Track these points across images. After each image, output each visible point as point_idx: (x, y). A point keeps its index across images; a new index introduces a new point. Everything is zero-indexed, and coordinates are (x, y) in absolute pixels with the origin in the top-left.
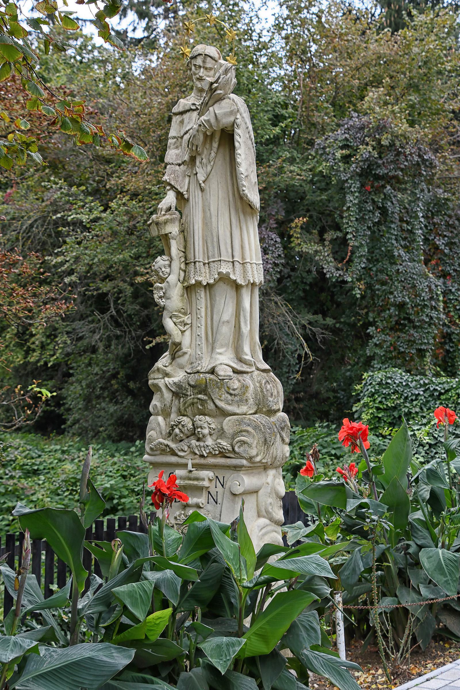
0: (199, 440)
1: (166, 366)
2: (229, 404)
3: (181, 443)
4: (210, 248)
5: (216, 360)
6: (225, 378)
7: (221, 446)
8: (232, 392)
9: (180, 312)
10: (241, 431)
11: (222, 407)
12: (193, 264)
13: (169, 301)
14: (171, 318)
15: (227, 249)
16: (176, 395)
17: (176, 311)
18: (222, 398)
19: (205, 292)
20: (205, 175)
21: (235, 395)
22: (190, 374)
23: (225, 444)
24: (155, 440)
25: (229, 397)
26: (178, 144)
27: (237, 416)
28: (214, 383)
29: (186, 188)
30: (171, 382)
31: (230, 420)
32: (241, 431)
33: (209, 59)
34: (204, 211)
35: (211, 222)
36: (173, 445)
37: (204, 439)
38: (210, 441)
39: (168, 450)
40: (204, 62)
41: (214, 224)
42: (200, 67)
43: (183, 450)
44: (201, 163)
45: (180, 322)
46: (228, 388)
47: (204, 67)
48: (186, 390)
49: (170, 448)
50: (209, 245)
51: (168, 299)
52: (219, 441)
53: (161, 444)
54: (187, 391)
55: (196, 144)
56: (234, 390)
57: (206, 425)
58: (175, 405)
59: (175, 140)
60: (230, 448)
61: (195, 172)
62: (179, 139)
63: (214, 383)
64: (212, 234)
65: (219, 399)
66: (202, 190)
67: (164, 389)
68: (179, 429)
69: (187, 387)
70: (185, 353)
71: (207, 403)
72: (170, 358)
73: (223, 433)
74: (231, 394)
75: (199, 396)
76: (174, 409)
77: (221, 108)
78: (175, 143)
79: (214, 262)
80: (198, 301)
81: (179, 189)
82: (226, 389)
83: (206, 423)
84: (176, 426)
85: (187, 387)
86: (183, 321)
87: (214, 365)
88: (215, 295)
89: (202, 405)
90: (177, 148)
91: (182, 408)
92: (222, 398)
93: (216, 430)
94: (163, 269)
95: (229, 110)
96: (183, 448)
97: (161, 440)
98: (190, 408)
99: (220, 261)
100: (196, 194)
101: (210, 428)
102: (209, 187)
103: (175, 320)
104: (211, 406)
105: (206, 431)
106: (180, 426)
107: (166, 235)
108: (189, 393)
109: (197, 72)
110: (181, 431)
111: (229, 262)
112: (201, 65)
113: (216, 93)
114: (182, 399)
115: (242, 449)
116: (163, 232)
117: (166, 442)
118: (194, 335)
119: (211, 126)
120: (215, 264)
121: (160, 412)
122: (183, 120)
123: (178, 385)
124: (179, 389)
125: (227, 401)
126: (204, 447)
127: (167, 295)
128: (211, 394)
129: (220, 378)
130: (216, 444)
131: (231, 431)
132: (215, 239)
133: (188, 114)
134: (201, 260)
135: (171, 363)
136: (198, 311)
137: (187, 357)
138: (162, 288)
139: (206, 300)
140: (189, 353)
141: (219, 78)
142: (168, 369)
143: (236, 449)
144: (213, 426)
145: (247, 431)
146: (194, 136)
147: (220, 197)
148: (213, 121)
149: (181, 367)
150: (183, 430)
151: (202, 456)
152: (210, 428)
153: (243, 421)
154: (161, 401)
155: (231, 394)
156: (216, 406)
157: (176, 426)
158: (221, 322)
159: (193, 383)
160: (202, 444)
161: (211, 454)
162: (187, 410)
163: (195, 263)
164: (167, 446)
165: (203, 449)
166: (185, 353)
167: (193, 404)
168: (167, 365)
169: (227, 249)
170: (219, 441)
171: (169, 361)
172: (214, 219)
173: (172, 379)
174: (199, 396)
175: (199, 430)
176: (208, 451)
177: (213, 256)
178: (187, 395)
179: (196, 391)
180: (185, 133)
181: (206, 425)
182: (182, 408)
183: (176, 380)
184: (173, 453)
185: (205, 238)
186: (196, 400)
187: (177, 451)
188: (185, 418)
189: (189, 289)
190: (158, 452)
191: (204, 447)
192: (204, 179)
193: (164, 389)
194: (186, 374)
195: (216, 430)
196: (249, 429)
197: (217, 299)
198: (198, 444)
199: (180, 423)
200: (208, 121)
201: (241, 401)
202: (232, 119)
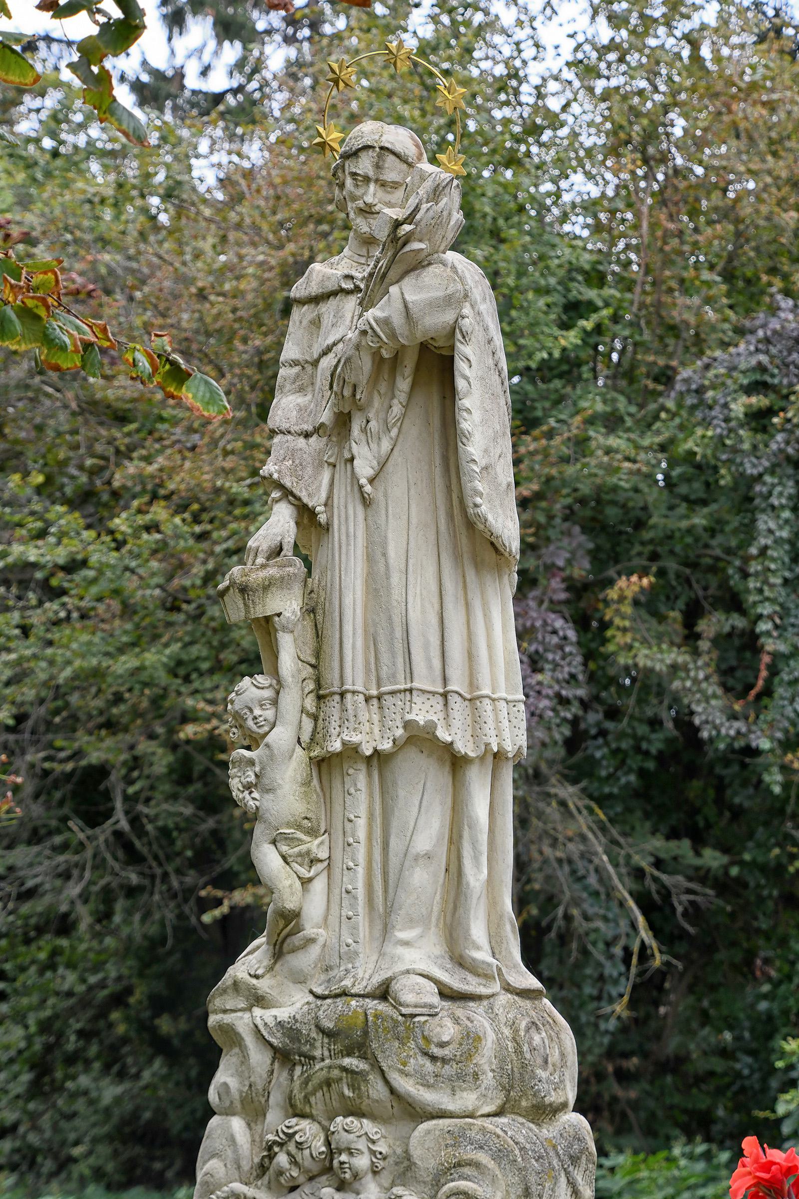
1: (256, 977)
2: (428, 1086)
4: (385, 658)
5: (394, 959)
8: (436, 1051)
9: (299, 827)
10: (459, 1165)
12: (337, 698)
13: (270, 796)
14: (274, 842)
15: (428, 660)
16: (283, 1056)
17: (288, 825)
18: (409, 1069)
19: (369, 775)
20: (375, 464)
21: (444, 1061)
25: (428, 1065)
26: (306, 380)
27: (447, 1121)
28: (389, 1024)
29: (323, 495)
31: (428, 1132)
32: (459, 1165)
33: (391, 158)
34: (370, 559)
35: (388, 588)
37: (356, 1185)
40: (378, 167)
41: (397, 594)
42: (367, 179)
44: (364, 430)
45: (300, 855)
46: (427, 1039)
47: (377, 181)
48: (312, 1043)
50: (383, 648)
54: (313, 1046)
56: (442, 1045)
57: (362, 1145)
58: (279, 1085)
59: (297, 369)
61: (347, 455)
62: (309, 368)
63: (389, 1024)
64: (390, 618)
65: (401, 1072)
66: (366, 502)
67: (249, 1041)
68: (289, 1154)
69: (314, 1035)
70: (312, 941)
71: (366, 1081)
72: (270, 953)
74: (433, 1058)
75: (347, 1061)
76: (276, 1098)
77: (421, 289)
78: (298, 376)
79: (392, 693)
81: (305, 500)
82: (421, 1041)
84: (281, 1145)
85: (314, 1035)
86: (308, 852)
87: (389, 974)
88: (395, 783)
89: (353, 1087)
90: (301, 390)
91: (299, 1096)
92: (409, 1069)
93: (391, 1160)
94: (257, 712)
95: (440, 294)
97: (238, 1187)
98: (319, 1094)
99: (411, 690)
101: (373, 1153)
102: (386, 496)
103: (284, 848)
105: (362, 1162)
106: (292, 1147)
107: (268, 619)
108: (317, 1053)
109: (359, 192)
110: (294, 1162)
111: (434, 693)
112: (371, 173)
113: (407, 248)
114: (298, 1070)
116: (259, 612)
119: (393, 335)
120: (398, 700)
121: (238, 1104)
122: (319, 317)
123: (289, 1030)
124: (292, 1040)
125: (423, 1077)
127: (265, 781)
128: (380, 1057)
129: (404, 1011)
131: (432, 1164)
132: (399, 633)
133: (333, 302)
134: (356, 688)
135: (271, 969)
136: (348, 826)
137: (314, 951)
138: (251, 763)
139: (371, 795)
140: (321, 941)
141: (417, 209)
142: (264, 985)
145: (477, 1165)
146: (348, 360)
147: (414, 520)
148: (398, 321)
149: (299, 979)
150: (299, 1158)
152: (373, 1153)
153: (464, 1135)
155: (433, 1058)
156: (392, 1091)
157: (281, 1145)
158: (410, 857)
159: (331, 1025)
162: (313, 1100)
163: (342, 695)
166: (312, 941)
167: (328, 1083)
168: (260, 972)
169: (428, 660)
171: (266, 962)
172: (396, 579)
173: (274, 1012)
174: (347, 1061)
175: (344, 1157)
177: (393, 678)
178: (313, 1058)
179: (338, 1047)
180: (325, 353)
181: (362, 1145)
182: (299, 1096)
183: (283, 1013)
185: (372, 630)
186: (336, 1073)
188: (305, 1124)
189: (326, 766)
192: (370, 472)
193: (249, 1041)
194: (311, 998)
195: (391, 1160)
196: (483, 1157)
197: (402, 793)
199: (291, 1136)
200: (385, 322)
201: (461, 1076)
202: (449, 317)
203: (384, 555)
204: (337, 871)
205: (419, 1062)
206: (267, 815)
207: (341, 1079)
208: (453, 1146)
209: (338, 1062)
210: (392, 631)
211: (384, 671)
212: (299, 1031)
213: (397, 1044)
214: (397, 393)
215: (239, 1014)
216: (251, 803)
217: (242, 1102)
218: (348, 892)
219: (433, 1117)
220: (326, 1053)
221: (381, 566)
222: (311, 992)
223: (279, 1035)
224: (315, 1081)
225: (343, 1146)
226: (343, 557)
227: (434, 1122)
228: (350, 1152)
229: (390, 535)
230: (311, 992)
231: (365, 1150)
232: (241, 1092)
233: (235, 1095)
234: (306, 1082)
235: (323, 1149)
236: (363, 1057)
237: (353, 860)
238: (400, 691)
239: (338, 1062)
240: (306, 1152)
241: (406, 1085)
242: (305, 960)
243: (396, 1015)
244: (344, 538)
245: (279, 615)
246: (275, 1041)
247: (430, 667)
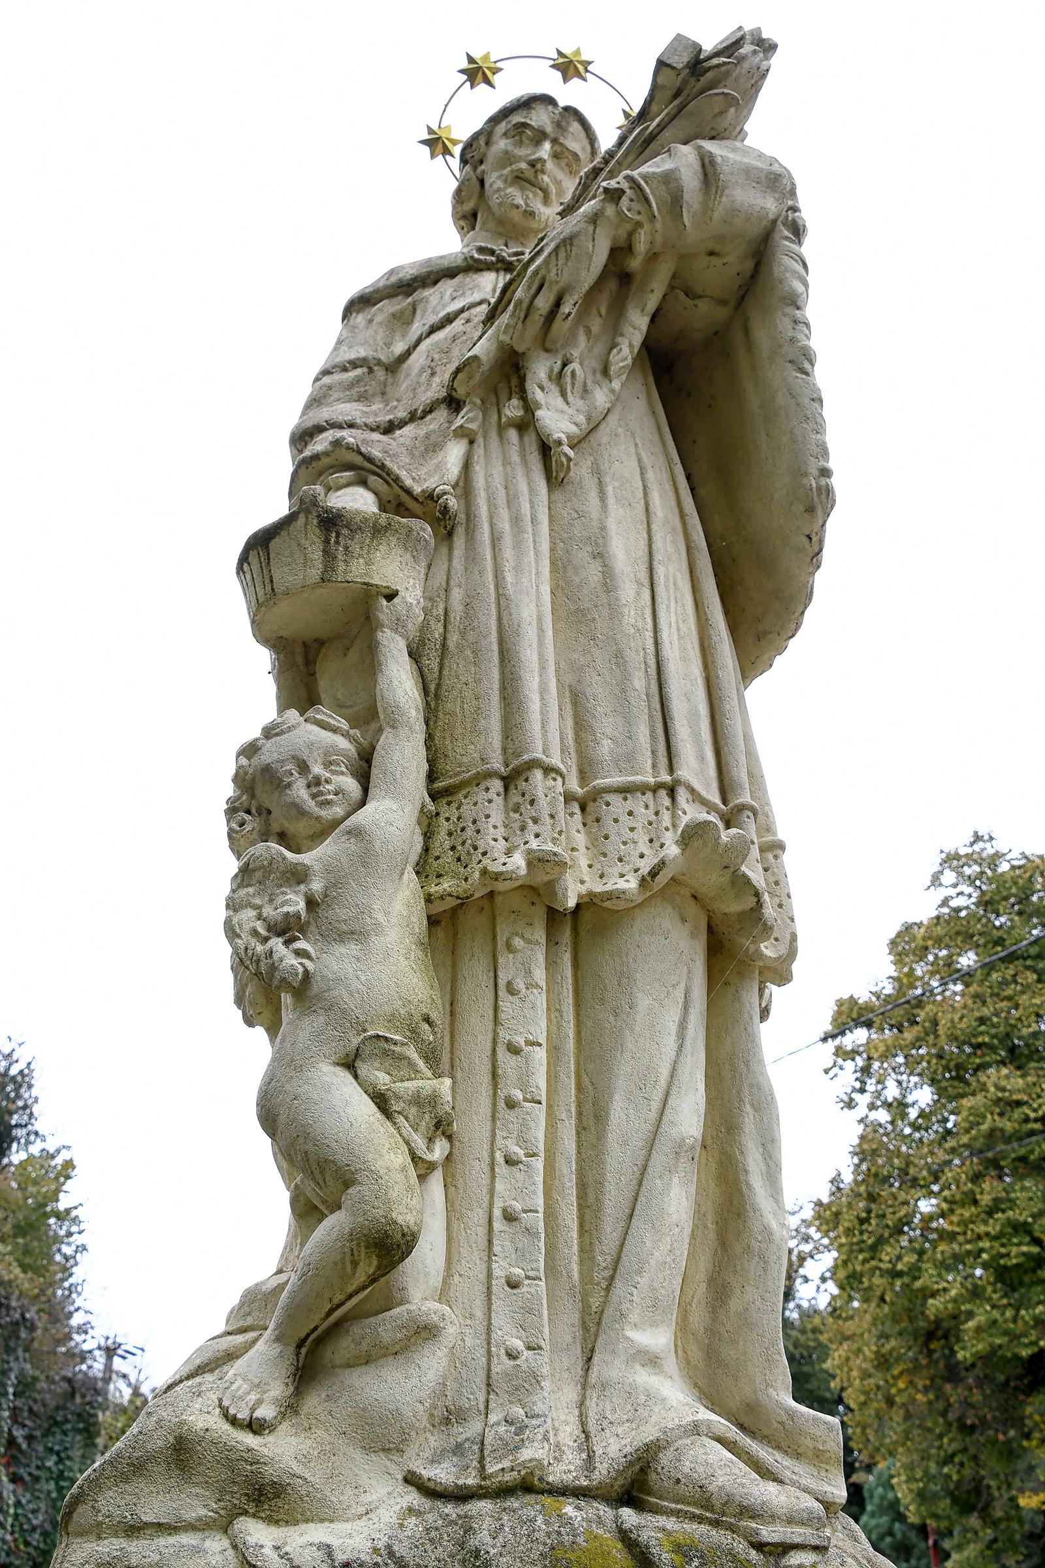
1: (255, 1426)
5: (639, 1403)
6: (797, 1534)
9: (414, 1034)
12: (497, 785)
13: (351, 949)
14: (350, 1064)
19: (551, 964)
20: (581, 419)
22: (461, 1496)
33: (575, 127)
34: (560, 566)
42: (540, 136)
45: (417, 1100)
47: (555, 141)
51: (343, 937)
55: (565, 278)
61: (513, 409)
62: (380, 373)
64: (618, 656)
70: (425, 1332)
78: (358, 380)
79: (625, 791)
80: (507, 1004)
87: (649, 1434)
90: (362, 398)
94: (317, 769)
100: (523, 487)
102: (597, 472)
103: (382, 1079)
112: (549, 129)
118: (478, 1216)
119: (675, 202)
127: (340, 912)
129: (770, 1533)
132: (640, 682)
134: (555, 760)
135: (290, 1408)
137: (432, 1364)
138: (298, 876)
139: (553, 1007)
142: (282, 1450)
148: (690, 179)
149: (381, 1437)
166: (425, 1332)
168: (266, 1412)
171: (278, 1389)
172: (630, 592)
173: (317, 1533)
180: (433, 329)
185: (568, 679)
194: (413, 1498)
197: (644, 1002)
200: (668, 178)
203: (601, 555)
204: (475, 1171)
206: (340, 992)
210: (626, 677)
211: (605, 749)
214: (627, 329)
216: (292, 961)
218: (510, 1217)
221: (593, 572)
222: (412, 1480)
226: (508, 553)
229: (611, 524)
230: (412, 1480)
237: (522, 1140)
238: (643, 789)
242: (405, 1386)
243: (741, 1546)
244: (505, 525)
245: (391, 596)
247: (702, 758)
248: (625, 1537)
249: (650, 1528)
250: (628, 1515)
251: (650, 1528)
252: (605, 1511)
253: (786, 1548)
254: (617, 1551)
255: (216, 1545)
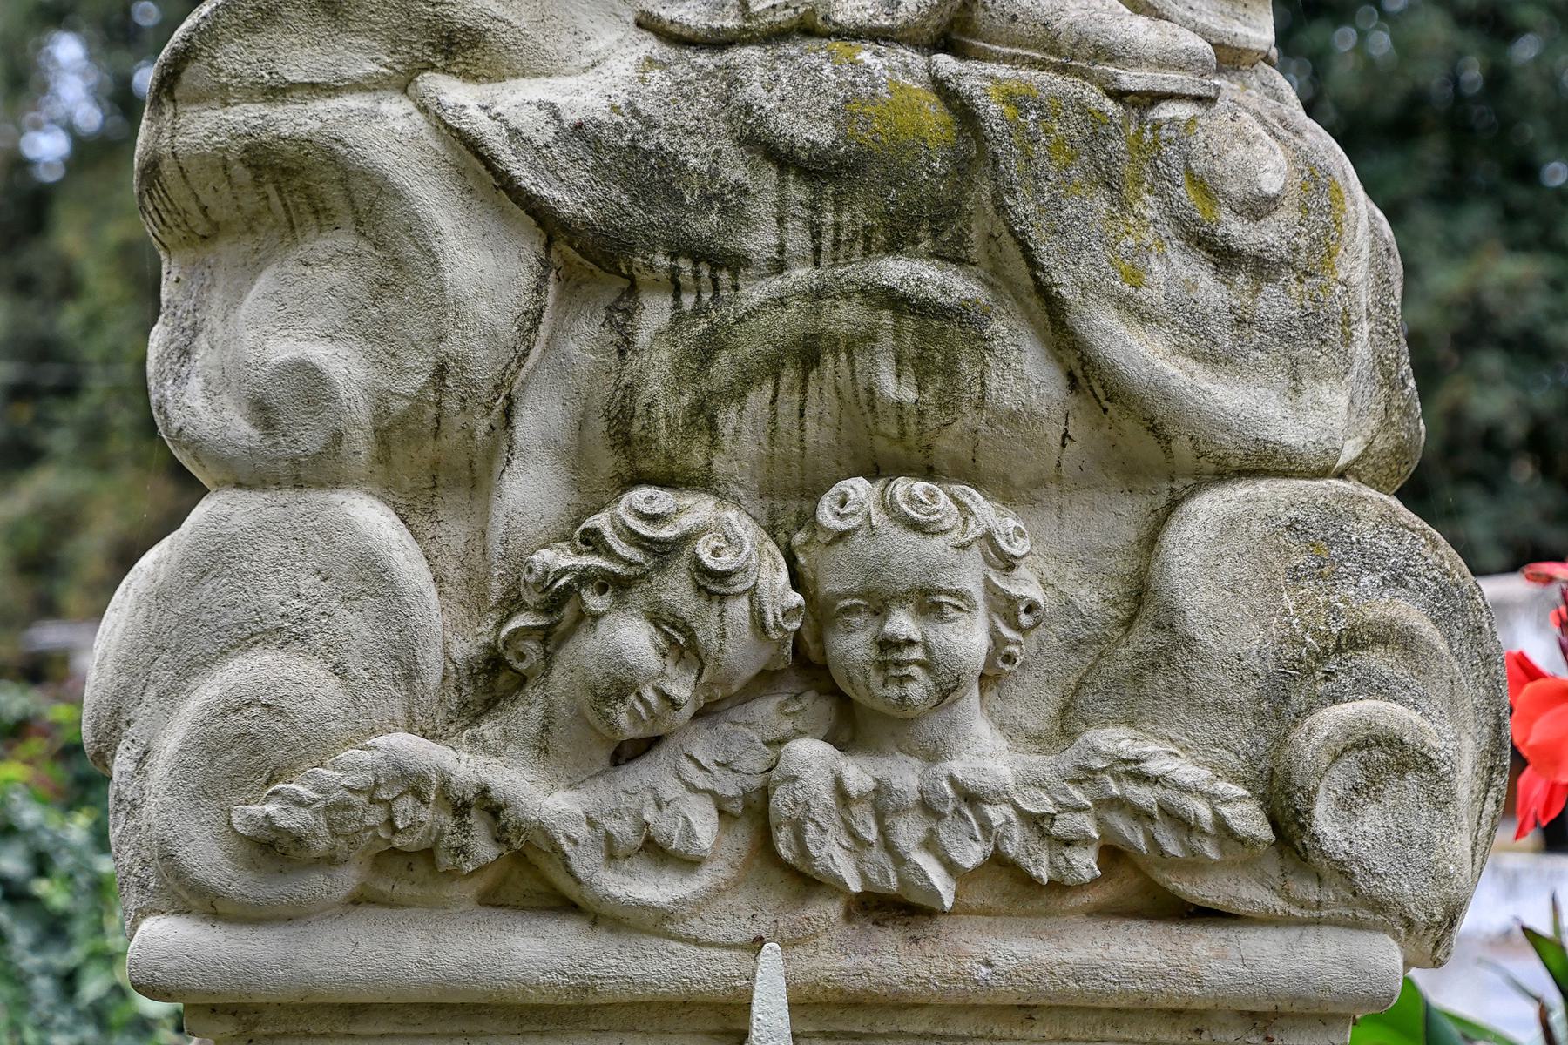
0: (852, 725)
2: (1213, 358)
3: (641, 774)
6: (1170, 81)
7: (1144, 796)
8: (1239, 231)
10: (1352, 641)
11: (1164, 391)
16: (588, 259)
18: (1153, 294)
21: (1262, 267)
22: (718, 42)
23: (1185, 770)
24: (320, 746)
25: (1210, 289)
28: (1074, 129)
30: (528, 121)
31: (1230, 525)
32: (1352, 641)
36: (550, 801)
37: (933, 727)
38: (986, 752)
39: (484, 849)
43: (656, 852)
46: (1204, 186)
49: (500, 836)
52: (1114, 739)
53: (414, 784)
56: (1258, 207)
57: (970, 577)
60: (1249, 819)
67: (435, 201)
68: (658, 618)
69: (736, 171)
71: (981, 343)
73: (1159, 660)
74: (1225, 258)
75: (895, 270)
76: (542, 416)
82: (1185, 195)
83: (977, 557)
85: (736, 171)
89: (921, 367)
93: (1053, 634)
96: (664, 826)
98: (757, 400)
101: (1007, 608)
104: (1022, 375)
105: (968, 638)
106: (676, 591)
108: (759, 241)
110: (682, 644)
114: (654, 313)
115: (1372, 820)
117: (462, 763)
121: (361, 444)
123: (628, 156)
124: (643, 194)
126: (928, 808)
130: (1085, 776)
143: (1325, 822)
144: (1026, 586)
145: (1403, 641)
150: (707, 634)
151: (893, 909)
152: (1007, 608)
154: (377, 335)
155: (1225, 258)
156: (1084, 373)
159: (822, 134)
160: (906, 776)
161: (1010, 886)
162: (728, 419)
164: (489, 806)
165: (908, 832)
170: (1114, 739)
173: (536, 89)
174: (895, 270)
175: (902, 624)
176: (972, 854)
178: (737, 262)
179: (857, 215)
181: (970, 577)
184: (532, 878)
186: (846, 315)
187: (587, 864)
188: (698, 510)
190: (348, 879)
191: (928, 808)
193: (435, 201)
194: (651, 46)
196: (1409, 612)
198: (858, 774)
199: (663, 552)
205: (1176, 272)
207: (870, 337)
208: (1317, 574)
209: (860, 271)
212: (669, 163)
213: (1100, 202)
215: (354, 102)
217: (382, 438)
219: (1225, 473)
220: (798, 241)
223: (579, 175)
224: (749, 348)
225: (904, 584)
227: (1240, 491)
228: (929, 603)
231: (978, 594)
232: (381, 402)
233: (359, 413)
234: (704, 353)
235: (797, 599)
236: (952, 255)
239: (860, 271)
240: (739, 610)
241: (1138, 351)
243: (1092, 95)
246: (564, 199)
248: (941, 87)
249: (972, 77)
250: (946, 63)
251: (972, 77)
252: (916, 60)
253: (1156, 98)
254: (933, 112)
255: (396, 109)
